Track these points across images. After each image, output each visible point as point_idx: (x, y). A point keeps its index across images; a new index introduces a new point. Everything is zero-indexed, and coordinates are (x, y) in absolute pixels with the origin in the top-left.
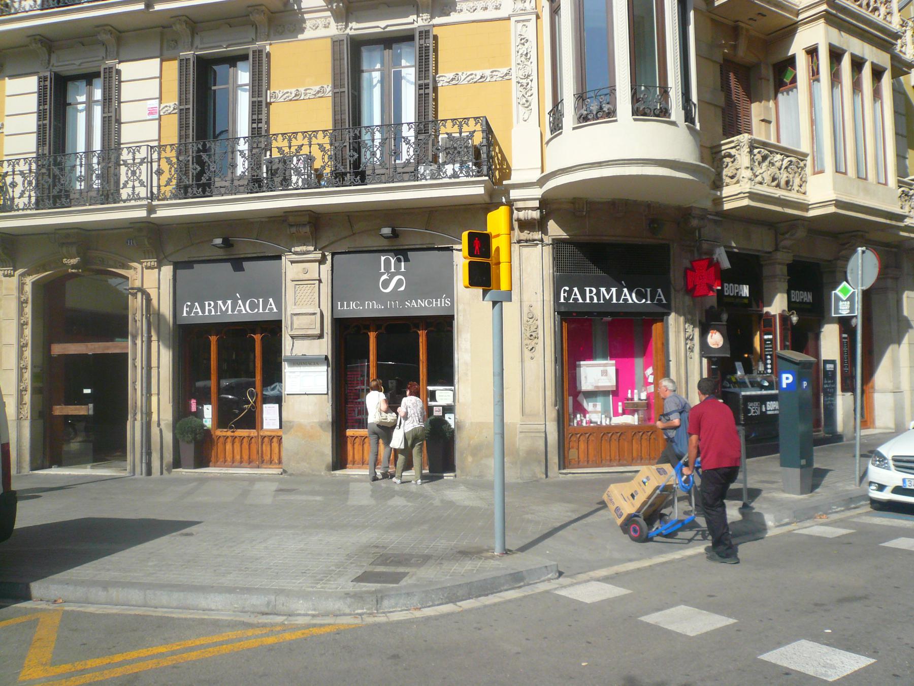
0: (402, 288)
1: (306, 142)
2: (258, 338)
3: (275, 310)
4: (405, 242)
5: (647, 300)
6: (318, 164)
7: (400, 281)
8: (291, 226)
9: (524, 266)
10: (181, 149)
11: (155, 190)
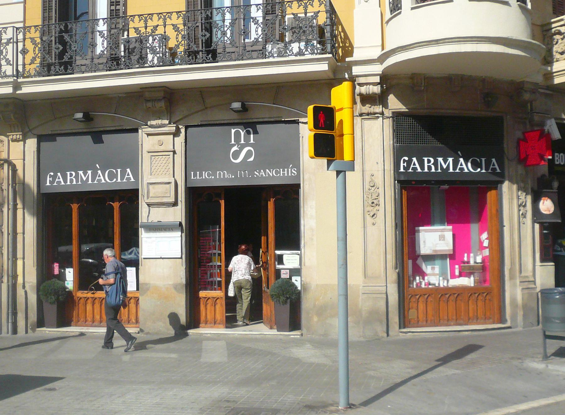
0: (252, 159)
1: (161, 22)
2: (116, 205)
3: (132, 180)
4: (254, 116)
5: (481, 169)
6: (172, 43)
8: (147, 101)
9: (366, 138)
10: (45, 30)
11: (20, 68)
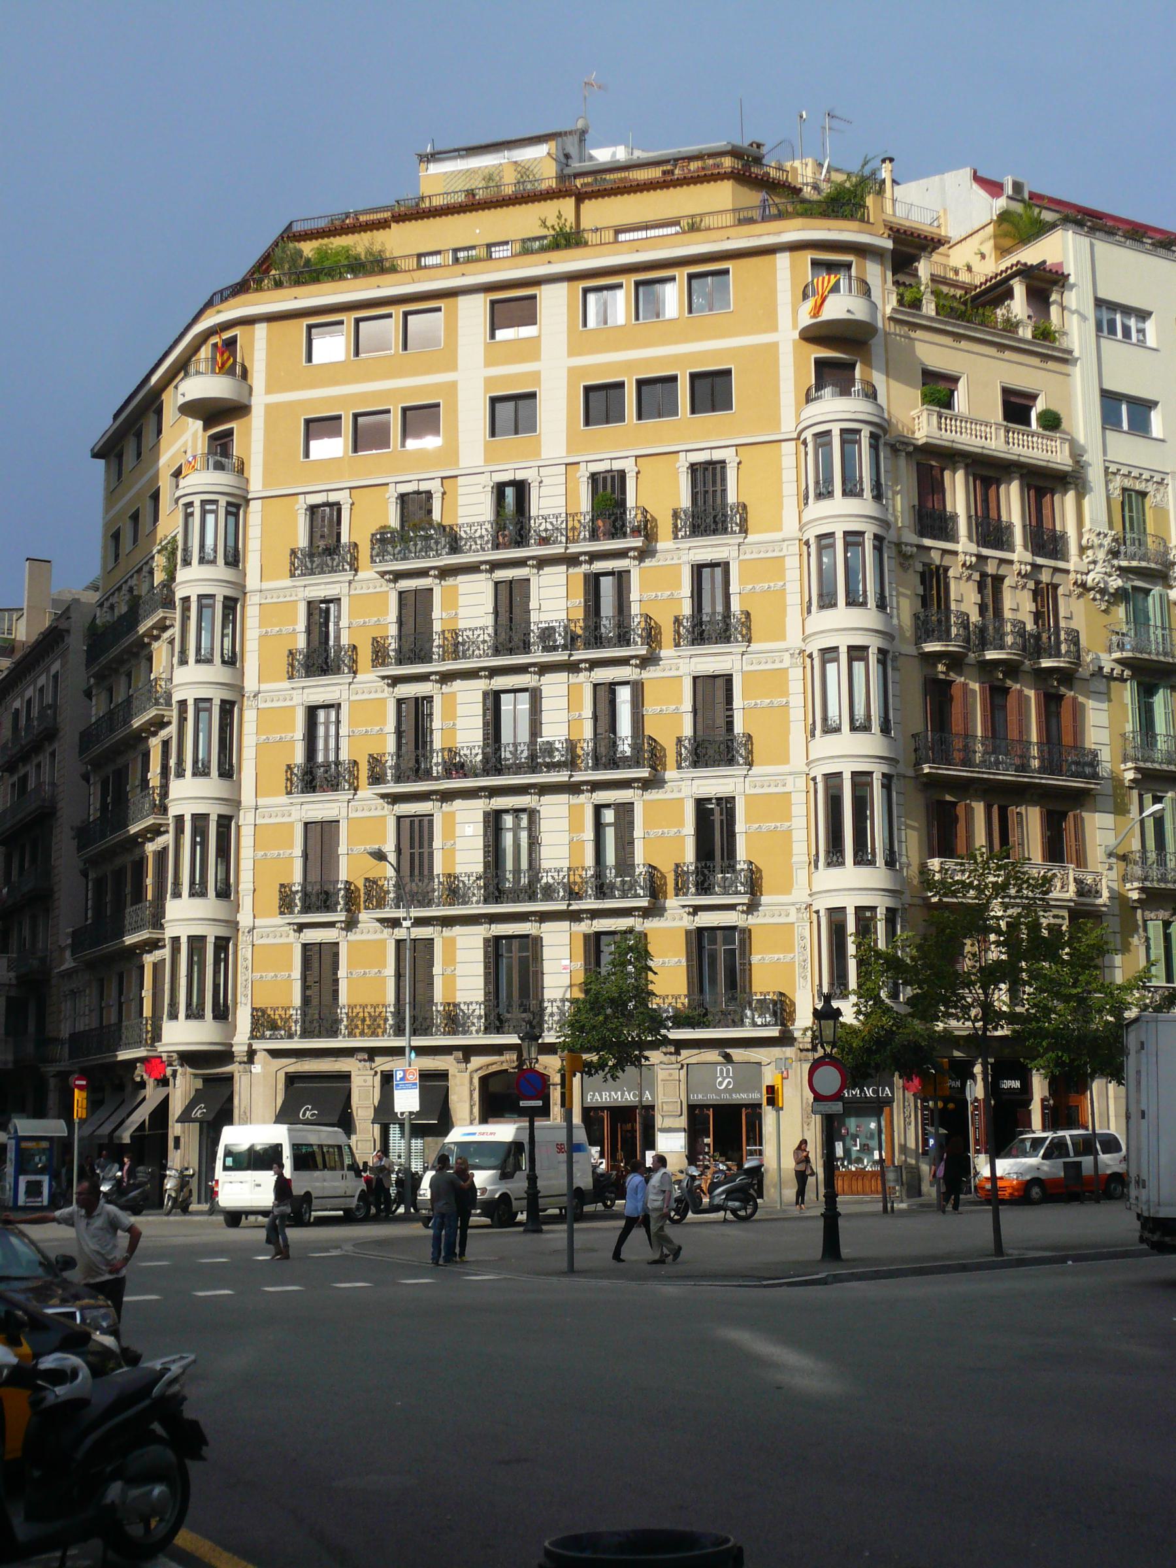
1: (674, 1000)
7: (729, 1082)
